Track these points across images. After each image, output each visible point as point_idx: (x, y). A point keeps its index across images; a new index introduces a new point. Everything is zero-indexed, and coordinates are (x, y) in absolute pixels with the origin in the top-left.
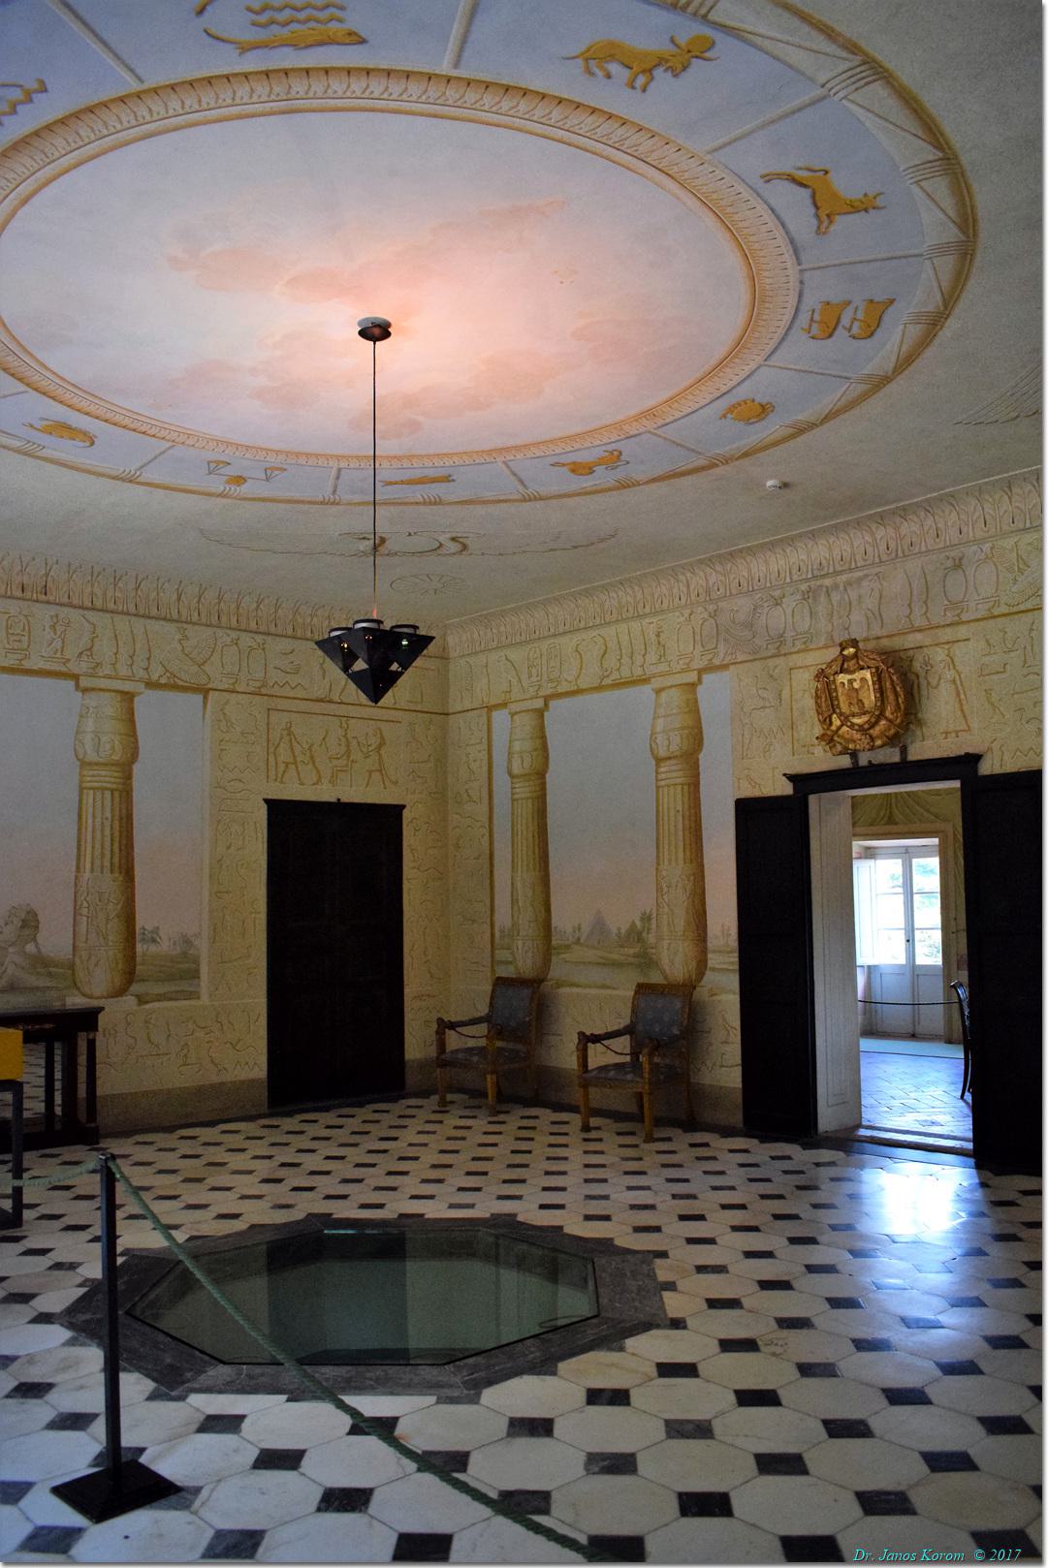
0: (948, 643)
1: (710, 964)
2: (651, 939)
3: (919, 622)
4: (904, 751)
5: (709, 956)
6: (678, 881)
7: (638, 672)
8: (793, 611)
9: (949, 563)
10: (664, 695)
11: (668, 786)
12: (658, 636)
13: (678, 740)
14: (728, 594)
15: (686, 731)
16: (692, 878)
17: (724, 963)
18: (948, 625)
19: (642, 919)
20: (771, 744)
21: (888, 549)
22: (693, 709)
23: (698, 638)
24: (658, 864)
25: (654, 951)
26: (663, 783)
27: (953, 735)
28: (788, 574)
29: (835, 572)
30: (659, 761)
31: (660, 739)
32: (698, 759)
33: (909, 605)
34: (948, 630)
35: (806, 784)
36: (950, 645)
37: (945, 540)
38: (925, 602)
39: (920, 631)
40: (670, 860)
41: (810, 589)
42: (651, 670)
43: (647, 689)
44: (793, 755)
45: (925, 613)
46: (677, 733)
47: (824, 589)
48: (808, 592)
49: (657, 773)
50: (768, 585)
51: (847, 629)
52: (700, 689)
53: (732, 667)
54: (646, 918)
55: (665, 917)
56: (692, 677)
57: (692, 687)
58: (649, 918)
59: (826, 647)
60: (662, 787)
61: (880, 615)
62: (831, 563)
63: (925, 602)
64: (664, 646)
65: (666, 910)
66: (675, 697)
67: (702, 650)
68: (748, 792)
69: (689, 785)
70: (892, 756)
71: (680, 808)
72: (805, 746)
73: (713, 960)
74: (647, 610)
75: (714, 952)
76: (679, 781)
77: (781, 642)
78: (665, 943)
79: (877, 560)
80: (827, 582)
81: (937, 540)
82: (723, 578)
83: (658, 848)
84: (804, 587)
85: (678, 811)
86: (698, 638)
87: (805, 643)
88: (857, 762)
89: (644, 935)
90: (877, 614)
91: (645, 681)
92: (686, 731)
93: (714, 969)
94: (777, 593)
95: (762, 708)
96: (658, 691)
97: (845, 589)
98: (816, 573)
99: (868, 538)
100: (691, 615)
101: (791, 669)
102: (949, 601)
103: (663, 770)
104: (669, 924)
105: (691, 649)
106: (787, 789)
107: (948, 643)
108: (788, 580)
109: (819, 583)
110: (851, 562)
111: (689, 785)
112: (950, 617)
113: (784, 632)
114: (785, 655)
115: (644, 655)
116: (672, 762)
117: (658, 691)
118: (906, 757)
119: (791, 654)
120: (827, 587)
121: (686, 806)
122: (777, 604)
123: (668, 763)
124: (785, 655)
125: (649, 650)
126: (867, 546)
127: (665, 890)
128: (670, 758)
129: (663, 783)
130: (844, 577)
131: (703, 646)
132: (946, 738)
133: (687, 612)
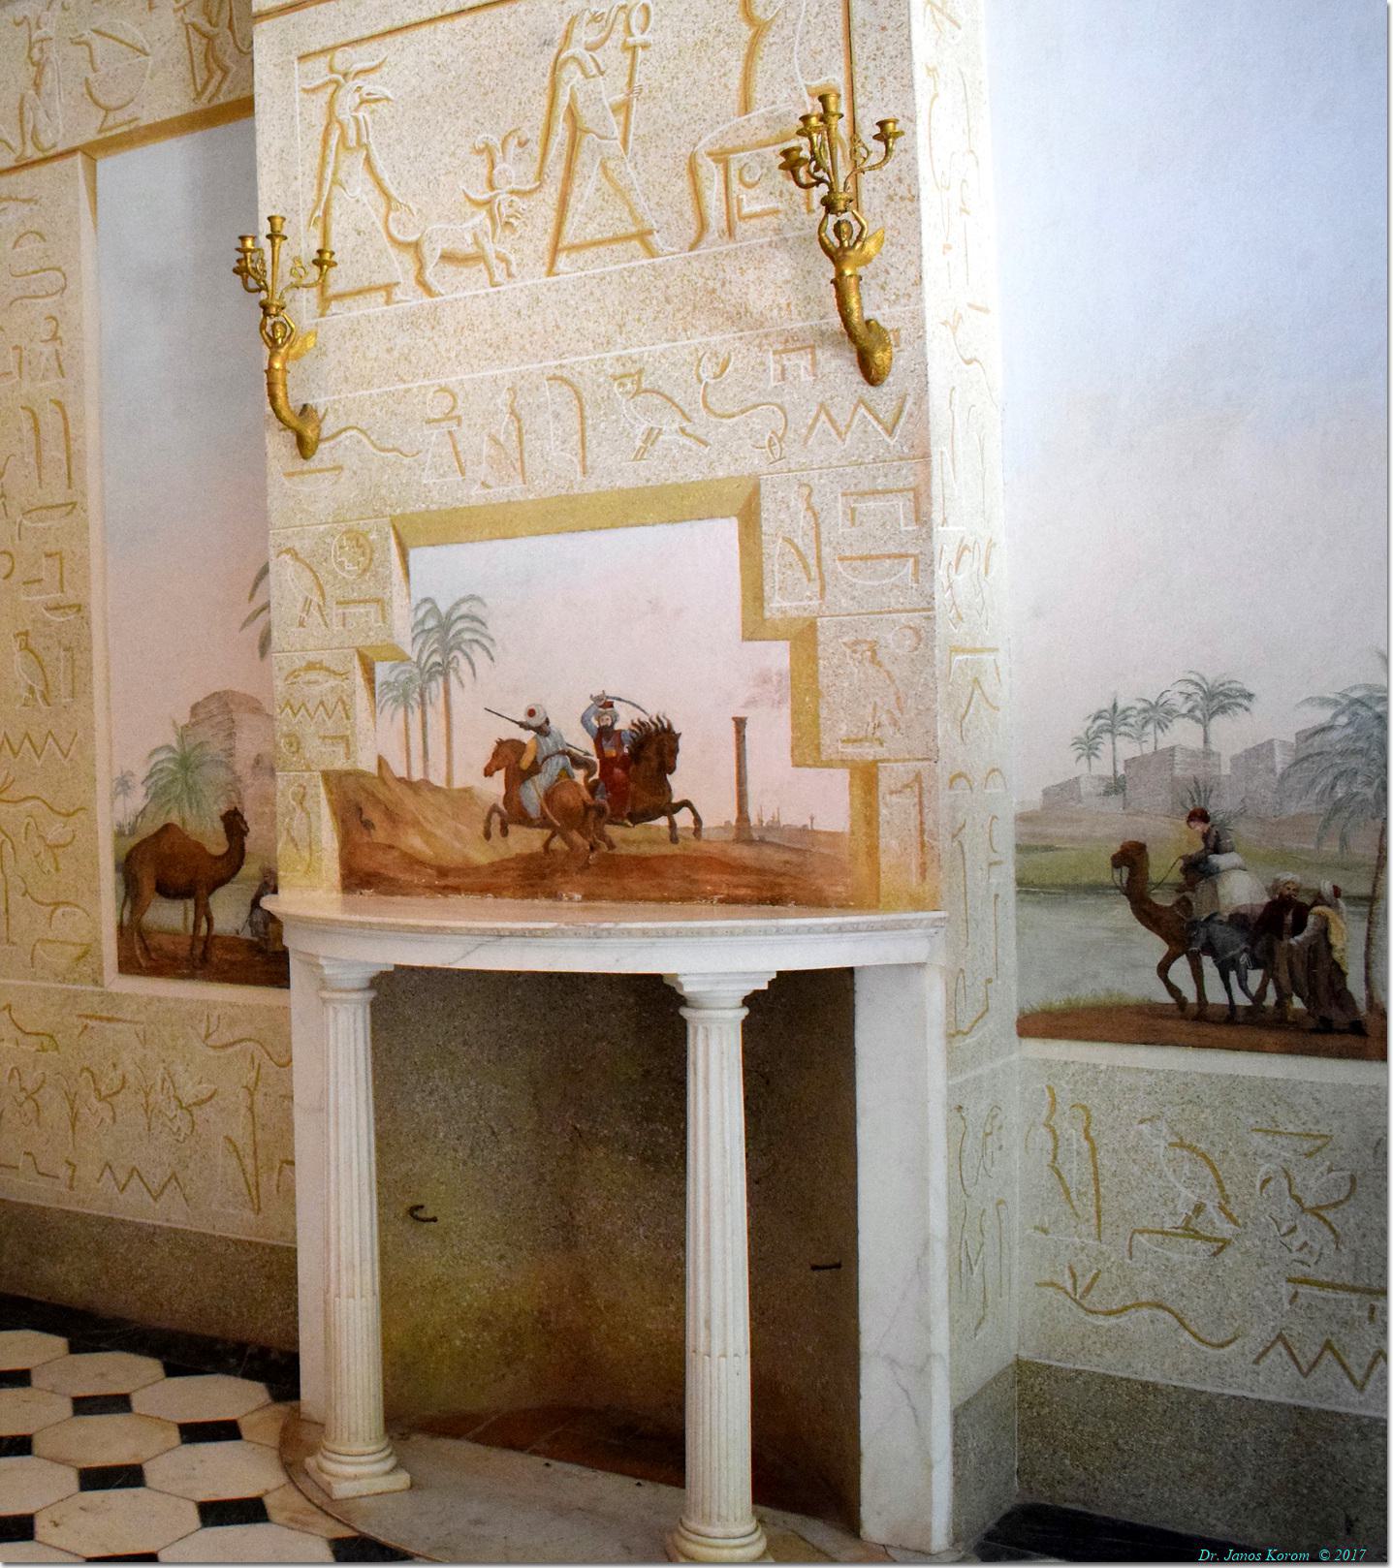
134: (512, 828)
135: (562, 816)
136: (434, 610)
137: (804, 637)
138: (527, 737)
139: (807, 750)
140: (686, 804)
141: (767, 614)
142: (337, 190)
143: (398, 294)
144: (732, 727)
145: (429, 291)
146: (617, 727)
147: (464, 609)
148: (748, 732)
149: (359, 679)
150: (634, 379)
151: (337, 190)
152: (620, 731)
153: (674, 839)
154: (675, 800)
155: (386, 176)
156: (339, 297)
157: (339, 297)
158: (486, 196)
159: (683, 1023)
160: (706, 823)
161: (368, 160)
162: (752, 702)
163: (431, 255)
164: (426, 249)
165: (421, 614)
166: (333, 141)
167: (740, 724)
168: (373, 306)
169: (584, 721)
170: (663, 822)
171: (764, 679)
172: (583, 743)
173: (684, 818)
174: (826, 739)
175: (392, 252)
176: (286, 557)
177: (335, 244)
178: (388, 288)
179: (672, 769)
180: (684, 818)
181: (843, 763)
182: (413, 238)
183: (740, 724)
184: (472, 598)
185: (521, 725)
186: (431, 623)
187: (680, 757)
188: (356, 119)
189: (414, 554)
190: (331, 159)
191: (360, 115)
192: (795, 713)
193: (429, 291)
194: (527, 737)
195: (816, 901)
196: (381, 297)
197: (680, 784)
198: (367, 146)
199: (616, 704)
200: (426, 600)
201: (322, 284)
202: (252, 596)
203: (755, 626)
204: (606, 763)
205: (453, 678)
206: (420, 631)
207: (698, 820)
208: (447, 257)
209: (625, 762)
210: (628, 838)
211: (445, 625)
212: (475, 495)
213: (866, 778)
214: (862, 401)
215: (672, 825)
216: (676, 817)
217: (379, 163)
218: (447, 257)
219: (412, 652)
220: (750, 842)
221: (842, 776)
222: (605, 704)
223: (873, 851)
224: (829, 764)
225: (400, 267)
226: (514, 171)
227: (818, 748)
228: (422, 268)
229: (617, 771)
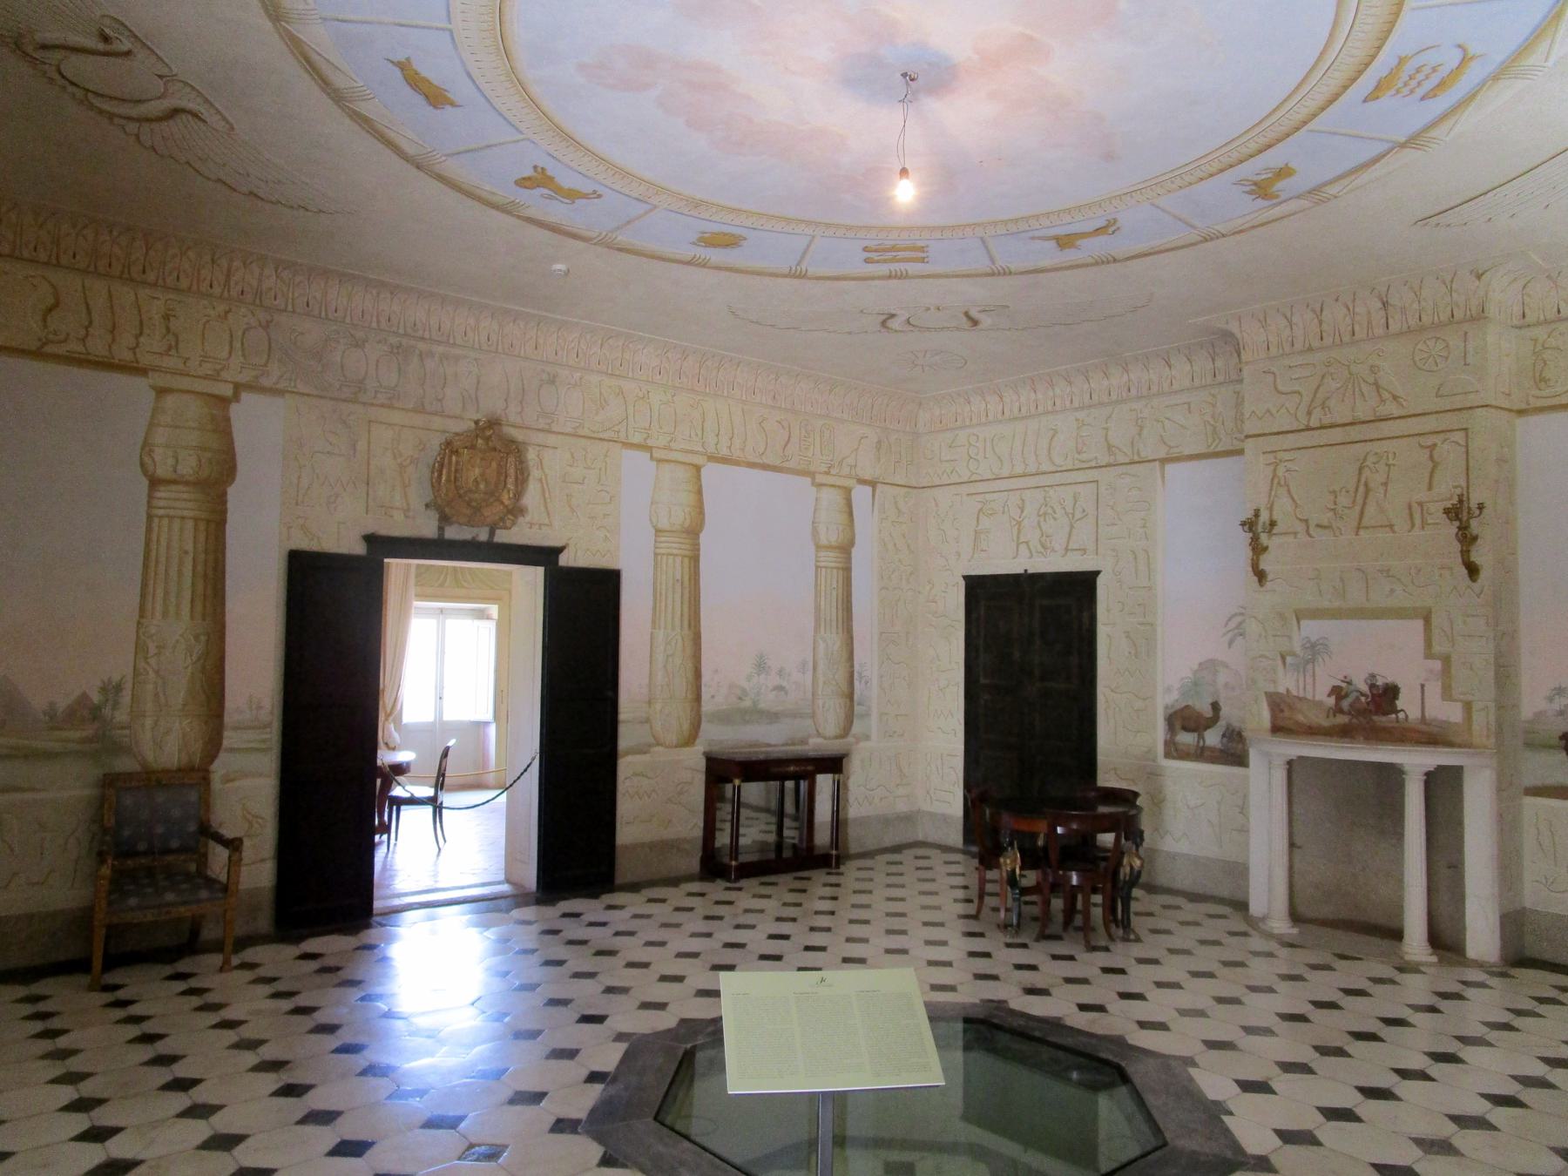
0: (540, 446)
1: (225, 743)
2: (121, 716)
3: (513, 418)
4: (492, 533)
5: (226, 734)
6: (177, 641)
7: (127, 356)
8: (378, 361)
9: (545, 376)
10: (170, 401)
11: (171, 518)
12: (167, 317)
13: (193, 462)
14: (290, 308)
15: (209, 455)
16: (203, 638)
17: (249, 742)
18: (539, 430)
19: (104, 690)
20: (337, 496)
21: (489, 340)
22: (223, 429)
23: (237, 345)
24: (141, 616)
25: (127, 732)
26: (161, 512)
27: (537, 527)
28: (375, 319)
29: (430, 339)
30: (155, 483)
31: (159, 453)
32: (224, 494)
33: (506, 400)
34: (541, 435)
35: (383, 546)
36: (541, 448)
37: (543, 355)
38: (521, 402)
39: (512, 426)
40: (165, 614)
41: (401, 344)
42: (145, 360)
43: (140, 384)
44: (367, 513)
45: (520, 413)
46: (191, 452)
47: (417, 352)
48: (398, 348)
49: (150, 497)
50: (348, 320)
51: (440, 400)
52: (234, 409)
53: (287, 396)
54: (112, 690)
55: (150, 687)
56: (227, 391)
57: (224, 402)
58: (118, 688)
59: (415, 410)
60: (161, 517)
61: (477, 398)
62: (427, 328)
63: (521, 402)
64: (176, 336)
65: (152, 675)
66: (194, 409)
67: (242, 359)
68: (304, 544)
69: (208, 521)
70: (483, 536)
71: (190, 547)
72: (382, 507)
73: (230, 738)
74: (151, 277)
75: (236, 729)
76: (191, 514)
77: (359, 387)
78: (149, 722)
79: (477, 346)
80: (421, 346)
81: (536, 352)
82: (285, 289)
83: (143, 596)
84: (393, 340)
85: (186, 552)
86: (237, 345)
87: (390, 399)
88: (443, 534)
89: (107, 712)
90: (474, 396)
91: (142, 371)
92: (209, 455)
93: (231, 750)
94: (360, 334)
95: (328, 453)
96: (161, 392)
97: (441, 360)
98: (409, 331)
99: (472, 321)
100: (227, 313)
101: (370, 421)
102: (542, 408)
103: (158, 494)
104: (156, 695)
105: (225, 354)
106: (359, 549)
107: (540, 446)
108: (374, 325)
109: (412, 342)
110: (449, 336)
111: (208, 521)
112: (542, 424)
113: (364, 379)
114: (364, 404)
115: (137, 337)
116: (180, 488)
117: (161, 392)
118: (493, 538)
119: (372, 405)
120: (421, 352)
121: (201, 546)
122: (357, 346)
123: (174, 487)
124: (364, 404)
125: (146, 331)
126: (468, 328)
127: (152, 649)
128: (174, 482)
129: (161, 512)
130: (440, 349)
131: (244, 355)
132: (531, 528)
133: (221, 308)
134: (1337, 715)
135: (1356, 711)
136: (1309, 641)
137: (1446, 660)
138: (1344, 685)
139: (1447, 694)
140: (1402, 710)
141: (1433, 652)
142: (1276, 499)
143: (1299, 536)
144: (1419, 687)
145: (1310, 536)
146: (1378, 684)
147: (1321, 642)
148: (1425, 688)
149: (1279, 662)
150: (1387, 572)
151: (1276, 499)
152: (1378, 686)
153: (1398, 722)
154: (1399, 709)
155: (1296, 497)
156: (1275, 534)
157: (1275, 534)
158: (1332, 507)
159: (1403, 780)
160: (1410, 717)
161: (1289, 491)
162: (1426, 680)
163: (1312, 524)
164: (1310, 522)
165: (1305, 642)
166: (1276, 481)
167: (1423, 686)
168: (1290, 539)
169: (1365, 681)
170: (1394, 716)
171: (1431, 671)
172: (1365, 688)
173: (1401, 715)
174: (1453, 692)
175: (1298, 522)
176: (1253, 619)
177: (1275, 517)
178: (1295, 534)
179: (1397, 699)
180: (1401, 715)
181: (1461, 701)
182: (1305, 518)
183: (1423, 686)
184: (1325, 638)
185: (1342, 681)
186: (1308, 645)
187: (1401, 695)
188: (1285, 477)
189: (1302, 622)
190: (1274, 488)
191: (1286, 474)
192: (1443, 684)
193: (1310, 536)
194: (1344, 685)
195: (1450, 744)
196: (1292, 536)
197: (1400, 704)
198: (1288, 486)
199: (1378, 677)
200: (1307, 638)
201: (1270, 532)
202: (1227, 624)
203: (1429, 655)
204: (1373, 694)
205: (1316, 663)
206: (1304, 647)
207: (1407, 716)
208: (1318, 526)
209: (1380, 696)
210: (1381, 720)
211: (1313, 646)
212: (1326, 604)
213: (1468, 707)
214: (1469, 587)
215: (1397, 717)
216: (1399, 714)
217: (1293, 490)
218: (1318, 526)
219: (1302, 655)
220: (1425, 724)
221: (1459, 705)
222: (1373, 676)
223: (1470, 729)
224: (1456, 701)
225: (1300, 527)
226: (1344, 500)
227: (1451, 696)
228: (1308, 528)
229: (1377, 699)
